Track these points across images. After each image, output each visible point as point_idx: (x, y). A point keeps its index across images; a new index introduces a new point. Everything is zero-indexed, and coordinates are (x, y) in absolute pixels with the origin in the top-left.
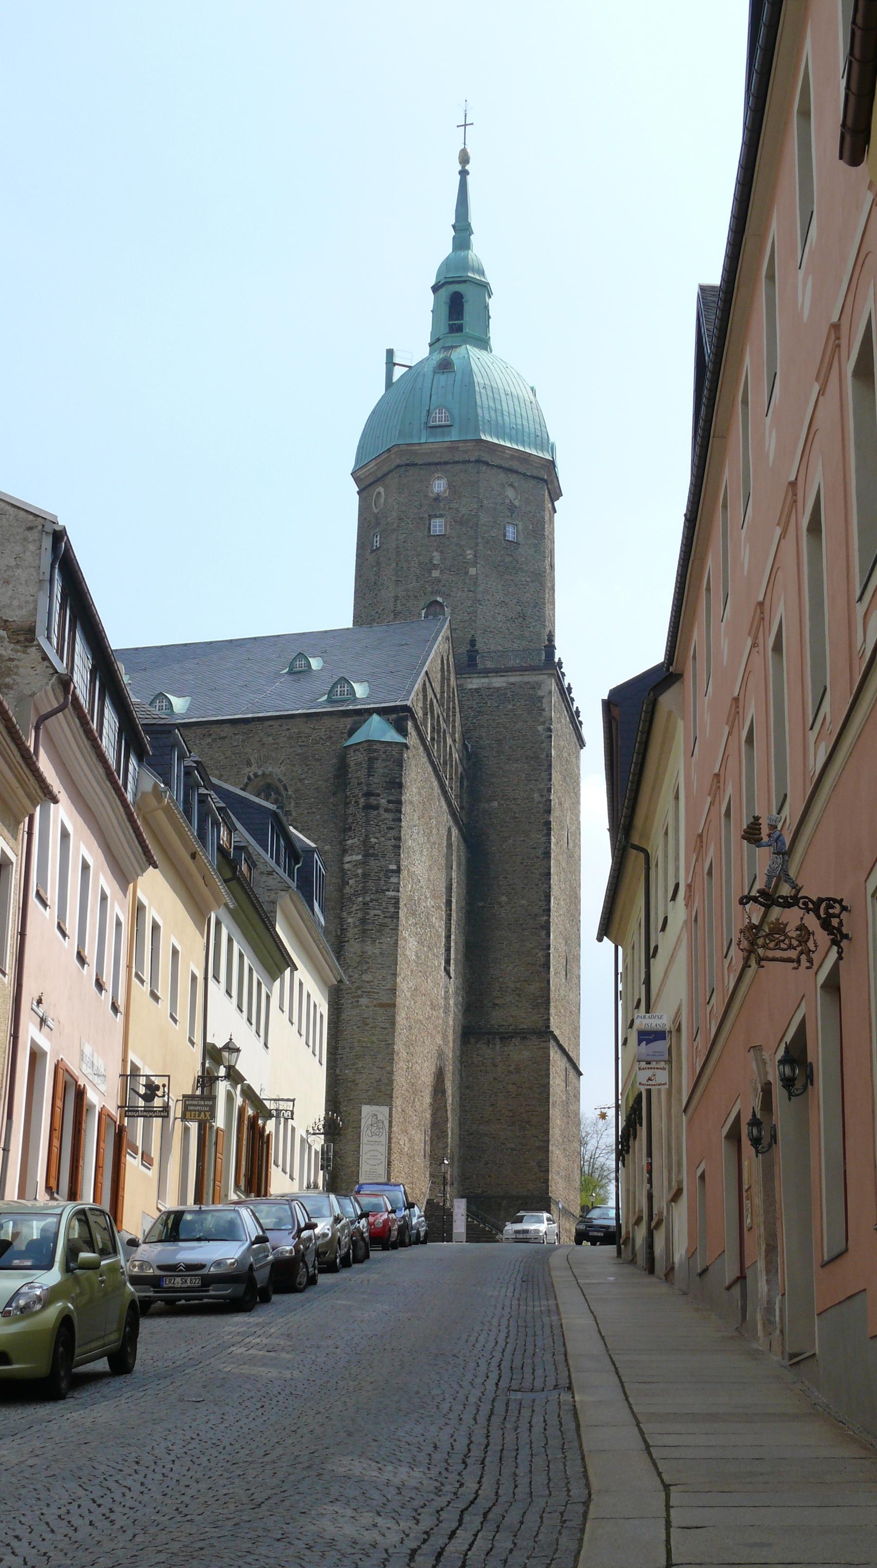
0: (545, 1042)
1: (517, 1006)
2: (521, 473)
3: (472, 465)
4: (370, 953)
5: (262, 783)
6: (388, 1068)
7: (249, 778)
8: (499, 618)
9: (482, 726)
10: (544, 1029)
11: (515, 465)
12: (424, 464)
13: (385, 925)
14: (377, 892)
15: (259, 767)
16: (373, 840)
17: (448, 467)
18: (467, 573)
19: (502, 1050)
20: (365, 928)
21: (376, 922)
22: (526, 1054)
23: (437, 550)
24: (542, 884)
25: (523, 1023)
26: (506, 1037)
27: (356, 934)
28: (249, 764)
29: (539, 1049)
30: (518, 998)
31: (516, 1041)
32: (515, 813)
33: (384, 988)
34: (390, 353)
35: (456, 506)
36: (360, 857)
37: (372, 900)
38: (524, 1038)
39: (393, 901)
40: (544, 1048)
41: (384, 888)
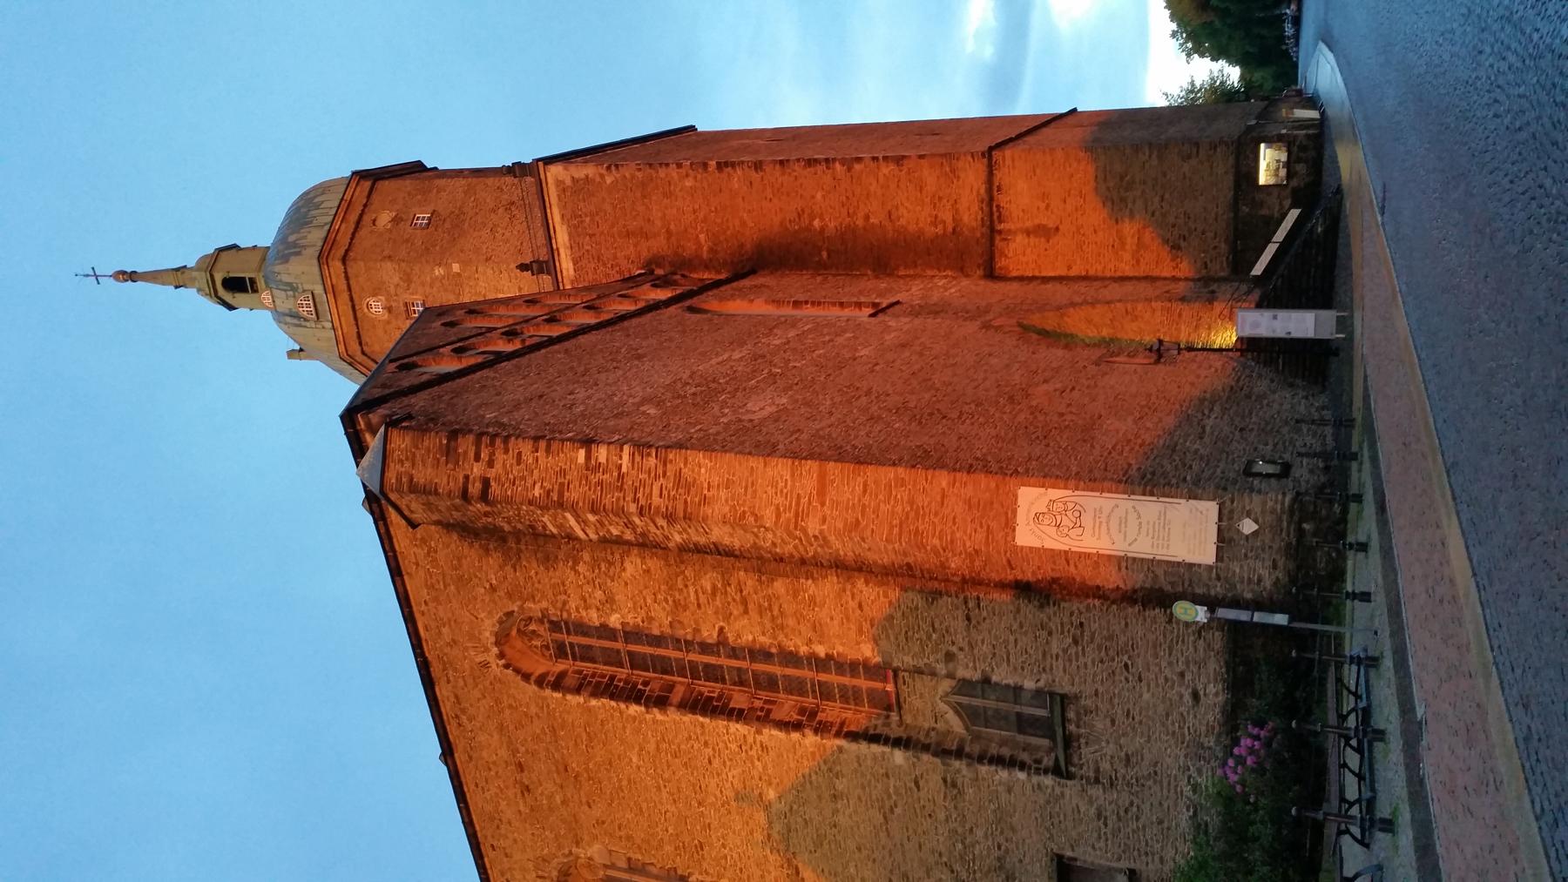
2: (363, 211)
4: (727, 509)
7: (507, 666)
8: (508, 234)
12: (357, 325)
13: (679, 475)
14: (621, 489)
15: (487, 650)
16: (537, 492)
18: (459, 275)
19: (1016, 219)
20: (682, 515)
21: (672, 493)
22: (1022, 185)
24: (795, 171)
25: (978, 192)
27: (697, 530)
28: (486, 665)
29: (1014, 167)
30: (945, 201)
31: (1002, 199)
33: (789, 483)
34: (291, 354)
35: (392, 287)
37: (636, 500)
38: (999, 189)
39: (638, 458)
40: (1013, 161)
41: (615, 474)
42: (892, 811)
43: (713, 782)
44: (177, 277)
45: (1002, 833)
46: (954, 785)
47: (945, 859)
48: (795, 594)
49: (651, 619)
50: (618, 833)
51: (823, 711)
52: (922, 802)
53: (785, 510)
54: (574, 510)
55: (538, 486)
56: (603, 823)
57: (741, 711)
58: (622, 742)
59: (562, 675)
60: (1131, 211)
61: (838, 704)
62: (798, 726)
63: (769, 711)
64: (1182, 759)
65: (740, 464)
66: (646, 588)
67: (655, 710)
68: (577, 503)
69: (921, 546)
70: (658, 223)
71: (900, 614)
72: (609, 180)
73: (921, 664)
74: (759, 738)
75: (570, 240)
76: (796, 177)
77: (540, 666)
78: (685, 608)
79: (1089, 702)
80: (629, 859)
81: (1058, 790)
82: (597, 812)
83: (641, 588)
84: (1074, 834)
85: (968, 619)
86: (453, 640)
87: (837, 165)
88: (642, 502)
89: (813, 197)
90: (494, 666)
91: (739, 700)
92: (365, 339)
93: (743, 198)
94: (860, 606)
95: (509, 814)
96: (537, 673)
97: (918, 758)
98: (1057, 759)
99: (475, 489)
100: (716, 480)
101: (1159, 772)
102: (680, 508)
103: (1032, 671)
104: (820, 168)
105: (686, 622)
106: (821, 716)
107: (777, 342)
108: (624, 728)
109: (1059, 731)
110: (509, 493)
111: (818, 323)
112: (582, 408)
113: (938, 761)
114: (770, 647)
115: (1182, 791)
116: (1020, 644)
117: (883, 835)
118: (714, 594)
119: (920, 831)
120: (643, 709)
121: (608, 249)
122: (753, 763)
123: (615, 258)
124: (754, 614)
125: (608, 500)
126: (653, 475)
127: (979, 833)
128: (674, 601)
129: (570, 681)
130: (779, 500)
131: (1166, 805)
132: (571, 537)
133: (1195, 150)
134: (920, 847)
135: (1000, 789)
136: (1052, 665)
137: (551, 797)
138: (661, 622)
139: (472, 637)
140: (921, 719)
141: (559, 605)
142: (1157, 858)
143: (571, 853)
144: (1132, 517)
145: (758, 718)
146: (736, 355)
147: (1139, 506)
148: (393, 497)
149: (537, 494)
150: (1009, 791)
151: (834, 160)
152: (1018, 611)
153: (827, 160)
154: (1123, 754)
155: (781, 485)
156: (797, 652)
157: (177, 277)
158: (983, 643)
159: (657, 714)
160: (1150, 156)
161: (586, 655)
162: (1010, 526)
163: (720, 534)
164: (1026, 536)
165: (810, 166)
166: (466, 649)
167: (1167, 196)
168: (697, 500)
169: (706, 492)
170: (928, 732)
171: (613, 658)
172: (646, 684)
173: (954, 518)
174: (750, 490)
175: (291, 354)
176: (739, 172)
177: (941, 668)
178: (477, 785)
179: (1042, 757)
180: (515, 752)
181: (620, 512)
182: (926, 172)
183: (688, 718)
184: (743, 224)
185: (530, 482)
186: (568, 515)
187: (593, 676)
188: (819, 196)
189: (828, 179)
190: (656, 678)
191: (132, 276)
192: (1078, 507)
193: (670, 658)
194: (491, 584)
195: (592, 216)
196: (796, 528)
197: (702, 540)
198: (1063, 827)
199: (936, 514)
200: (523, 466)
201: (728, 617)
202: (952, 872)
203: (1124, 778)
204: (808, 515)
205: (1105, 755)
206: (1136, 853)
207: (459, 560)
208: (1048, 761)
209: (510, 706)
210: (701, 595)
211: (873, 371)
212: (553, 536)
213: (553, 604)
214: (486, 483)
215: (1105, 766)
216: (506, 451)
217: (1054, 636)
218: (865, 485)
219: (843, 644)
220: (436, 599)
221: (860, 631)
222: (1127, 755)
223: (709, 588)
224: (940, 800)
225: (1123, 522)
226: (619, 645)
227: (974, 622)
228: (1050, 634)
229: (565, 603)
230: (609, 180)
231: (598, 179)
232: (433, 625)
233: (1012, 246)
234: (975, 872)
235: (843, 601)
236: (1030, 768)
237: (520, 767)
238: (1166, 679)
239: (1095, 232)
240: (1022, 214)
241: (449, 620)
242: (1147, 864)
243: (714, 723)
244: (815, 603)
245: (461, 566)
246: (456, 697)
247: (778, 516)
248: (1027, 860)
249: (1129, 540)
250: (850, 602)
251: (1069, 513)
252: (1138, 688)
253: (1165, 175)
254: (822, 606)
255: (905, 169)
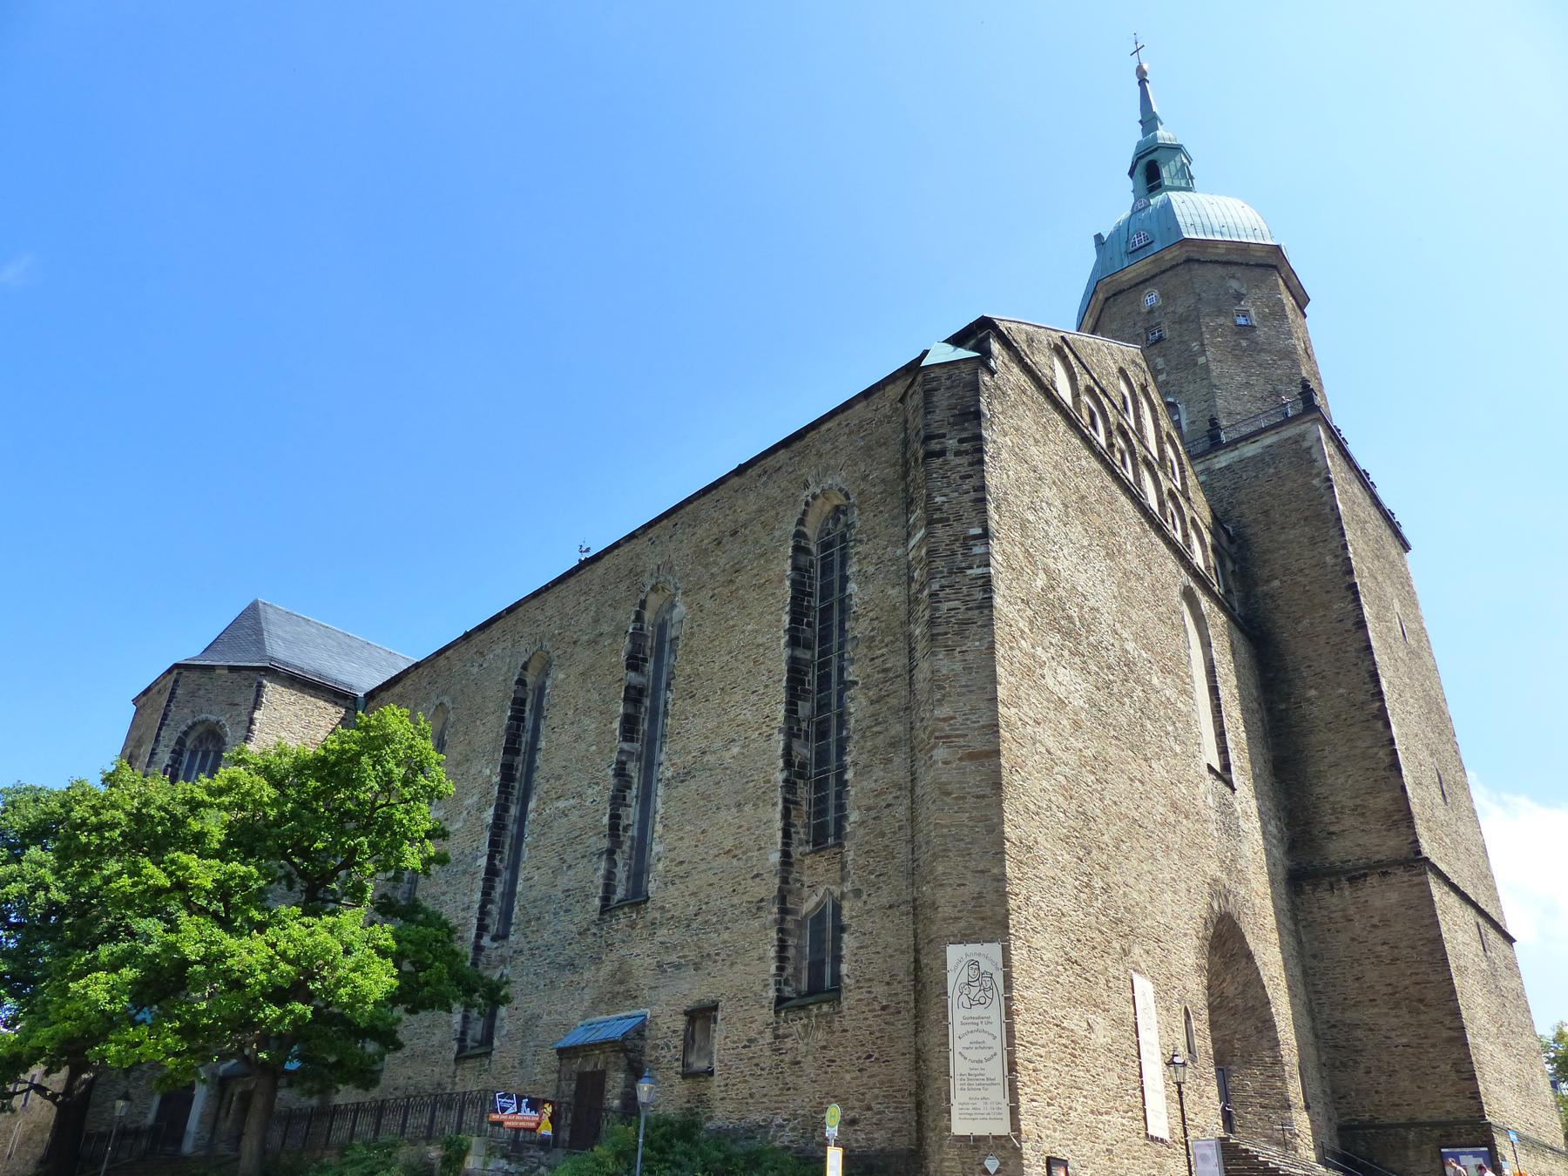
0: (1420, 874)
1: (1363, 831)
2: (1242, 264)
3: (1181, 267)
5: (828, 508)
6: (995, 871)
7: (807, 504)
9: (1240, 504)
10: (1412, 856)
11: (1234, 258)
14: (951, 573)
15: (817, 484)
17: (1157, 279)
18: (1196, 364)
20: (935, 632)
22: (1393, 897)
23: (1159, 356)
24: (1363, 661)
25: (1378, 852)
26: (1356, 875)
29: (1410, 886)
31: (1373, 880)
32: (1305, 586)
33: (976, 725)
34: (1098, 237)
35: (1173, 309)
36: (923, 531)
37: (943, 588)
38: (1385, 874)
39: (980, 582)
40: (1418, 884)
41: (964, 565)
42: (735, 856)
43: (738, 697)
44: (1149, 121)
45: (729, 956)
46: (759, 909)
47: (704, 907)
48: (892, 745)
49: (857, 619)
50: (695, 625)
51: (805, 784)
52: (743, 882)
53: (951, 725)
54: (929, 535)
55: (944, 499)
56: (701, 611)
57: (796, 712)
58: (761, 614)
59: (807, 551)
60: (1386, 1014)
61: (813, 796)
62: (788, 764)
63: (798, 736)
64: (803, 1112)
65: (987, 676)
66: (881, 609)
67: (787, 637)
68: (933, 537)
69: (935, 856)
70: (1283, 538)
71: (887, 842)
72: (1315, 482)
73: (850, 867)
74: (776, 731)
75: (1249, 458)
76: (1357, 664)
77: (811, 530)
78: (869, 648)
79: (837, 1024)
80: (677, 638)
81: (765, 1003)
82: (708, 604)
83: (881, 605)
84: (734, 1020)
85: (890, 907)
86: (821, 455)
87: (1378, 704)
88: (942, 594)
89: (1339, 685)
90: (806, 493)
91: (804, 709)
92: (1120, 298)
93: (1324, 616)
94: (888, 806)
95: (700, 532)
96: (805, 530)
97: (776, 874)
98: (791, 999)
99: (935, 445)
100: (970, 657)
101: (788, 1092)
102: (941, 629)
103: (856, 970)
104: (1370, 686)
105: (859, 651)
106: (800, 783)
107: (1155, 681)
108: (772, 613)
109: (811, 1000)
110: (934, 475)
111: (1189, 715)
112: (1031, 518)
113: (776, 893)
114: (847, 729)
115: (777, 1114)
116: (877, 955)
117: (715, 851)
118: (885, 671)
119: (722, 883)
120: (787, 626)
121: (1246, 495)
122: (756, 730)
123: (1240, 504)
124: (871, 709)
125: (939, 564)
126: (967, 598)
127: (726, 936)
128: (873, 637)
129: (803, 560)
130: (960, 719)
131: (764, 1100)
132: (909, 536)
133: (1464, 1076)
134: (710, 885)
135: (761, 951)
136: (862, 988)
137: (715, 562)
138: (858, 628)
139: (826, 469)
140: (809, 872)
141: (859, 537)
142: (724, 1094)
143: (677, 589)
144: (988, 1054)
145: (791, 728)
146: (1130, 646)
147: (998, 1059)
148: (920, 378)
149: (936, 500)
150: (759, 959)
151: (1383, 700)
152: (903, 952)
153: (1381, 693)
154: (799, 1059)
155: (974, 718)
156: (845, 754)
157: (1149, 121)
158: (873, 922)
159: (784, 640)
160: (1450, 1029)
161: (827, 568)
162: (964, 939)
163: (923, 670)
164: (956, 954)
165: (1371, 677)
166: (816, 466)
167: (1410, 1050)
168: (950, 643)
169: (958, 650)
170: (799, 880)
171: (826, 593)
172: (809, 624)
173: (963, 885)
174: (964, 689)
175: (1098, 237)
176: (1350, 607)
177: (848, 887)
178: (718, 501)
179: (791, 986)
180: (745, 526)
181: (931, 576)
182: (1388, 795)
183: (784, 667)
184: (1298, 621)
185: (947, 491)
186: (923, 531)
187: (809, 578)
188: (1342, 691)
189: (1362, 697)
190: (814, 632)
191: (1142, 82)
192: (988, 1001)
193: (831, 641)
194: (868, 475)
195: (1275, 474)
196: (936, 738)
197: (918, 655)
198: (739, 1009)
199: (966, 867)
200: (960, 482)
201: (866, 687)
202: (696, 915)
203: (782, 1061)
204: (950, 747)
205: (798, 1043)
206: (726, 1076)
207: (884, 444)
208: (788, 991)
209: (778, 514)
210: (881, 659)
211: (1131, 780)
212: (908, 521)
213: (860, 532)
214: (941, 453)
215: (789, 1043)
216: (970, 464)
217: (886, 987)
218: (983, 797)
219: (856, 795)
220: (851, 433)
221: (869, 809)
222: (799, 1063)
223: (888, 665)
224: (745, 898)
225: (980, 1045)
226: (837, 594)
227: (888, 912)
228: (888, 984)
229: (861, 541)
230: (1315, 482)
231: (1314, 471)
232: (832, 435)
233: (1327, 895)
234: (697, 935)
235: (891, 790)
236: (780, 975)
237: (734, 533)
238: (863, 1094)
239: (1358, 979)
240: (1362, 900)
241: (837, 447)
242: (719, 1086)
243: (783, 690)
244: (886, 764)
245: (880, 446)
246: (780, 467)
247: (944, 720)
248: (711, 980)
249: (966, 1053)
250: (891, 796)
251: (982, 993)
252: (853, 1068)
253: (1433, 1046)
254: (884, 770)
255: (1387, 774)
